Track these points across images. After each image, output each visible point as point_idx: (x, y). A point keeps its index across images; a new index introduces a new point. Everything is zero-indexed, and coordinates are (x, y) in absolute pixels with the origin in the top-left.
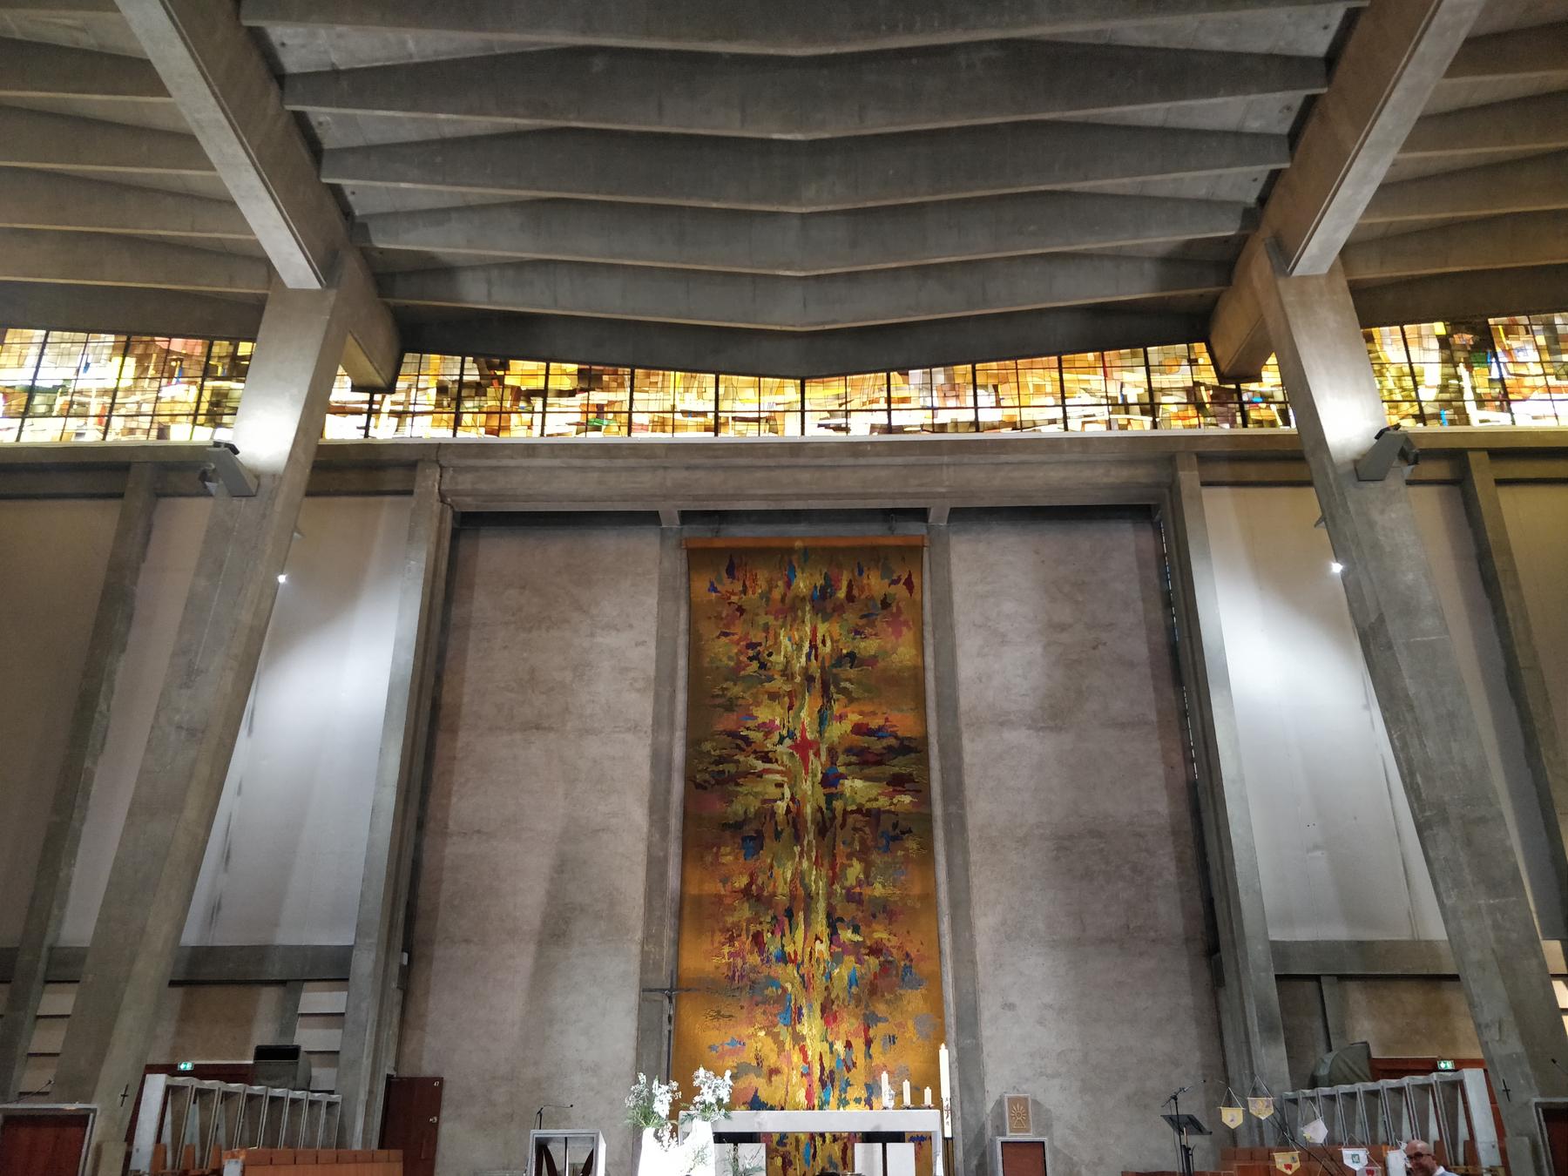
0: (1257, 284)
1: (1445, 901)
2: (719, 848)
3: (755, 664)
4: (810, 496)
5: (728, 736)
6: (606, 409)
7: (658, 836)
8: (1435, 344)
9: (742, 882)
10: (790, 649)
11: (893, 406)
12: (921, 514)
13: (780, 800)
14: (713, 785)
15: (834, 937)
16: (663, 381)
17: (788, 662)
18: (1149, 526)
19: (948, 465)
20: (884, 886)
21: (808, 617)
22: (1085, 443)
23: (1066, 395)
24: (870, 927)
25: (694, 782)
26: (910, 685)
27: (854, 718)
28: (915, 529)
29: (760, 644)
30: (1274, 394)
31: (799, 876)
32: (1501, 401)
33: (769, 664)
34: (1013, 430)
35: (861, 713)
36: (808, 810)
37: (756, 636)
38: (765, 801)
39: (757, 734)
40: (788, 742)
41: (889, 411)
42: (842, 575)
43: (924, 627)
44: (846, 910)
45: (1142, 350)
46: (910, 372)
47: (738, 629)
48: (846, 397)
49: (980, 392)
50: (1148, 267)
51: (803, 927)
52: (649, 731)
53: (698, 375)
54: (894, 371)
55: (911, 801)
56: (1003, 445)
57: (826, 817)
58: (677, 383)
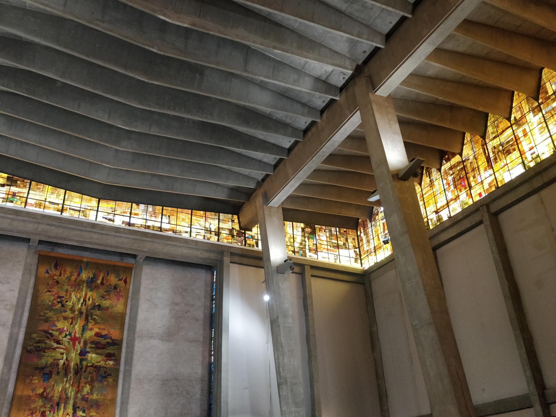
0: (257, 204)
1: (283, 409)
2: (33, 376)
3: (60, 305)
4: (95, 244)
5: (44, 332)
6: (16, 195)
7: (6, 370)
8: (300, 230)
9: (41, 391)
10: (75, 300)
11: (132, 216)
12: (134, 256)
13: (61, 359)
14: (34, 352)
15: (75, 414)
16: (43, 188)
17: (73, 305)
18: (210, 272)
19: (149, 241)
20: (97, 395)
21: (84, 289)
22: (197, 242)
23: (192, 224)
24: (89, 410)
25: (26, 349)
26: (119, 320)
27: (96, 330)
28: (131, 261)
29: (63, 297)
30: (255, 236)
31: (64, 390)
32: (315, 251)
33: (66, 305)
34: (173, 232)
35: (99, 329)
36: (72, 364)
37: (62, 294)
38: (55, 360)
39: (56, 332)
40: (68, 337)
41: (130, 217)
42: (100, 275)
43: (128, 298)
44: (83, 404)
45: (218, 214)
46: (140, 205)
47: (55, 290)
48: (115, 209)
49: (163, 217)
50: (226, 190)
51: (63, 409)
52: (10, 327)
53: (58, 189)
54: (134, 203)
55: (113, 364)
56: (169, 238)
57: (79, 367)
58: (49, 190)
